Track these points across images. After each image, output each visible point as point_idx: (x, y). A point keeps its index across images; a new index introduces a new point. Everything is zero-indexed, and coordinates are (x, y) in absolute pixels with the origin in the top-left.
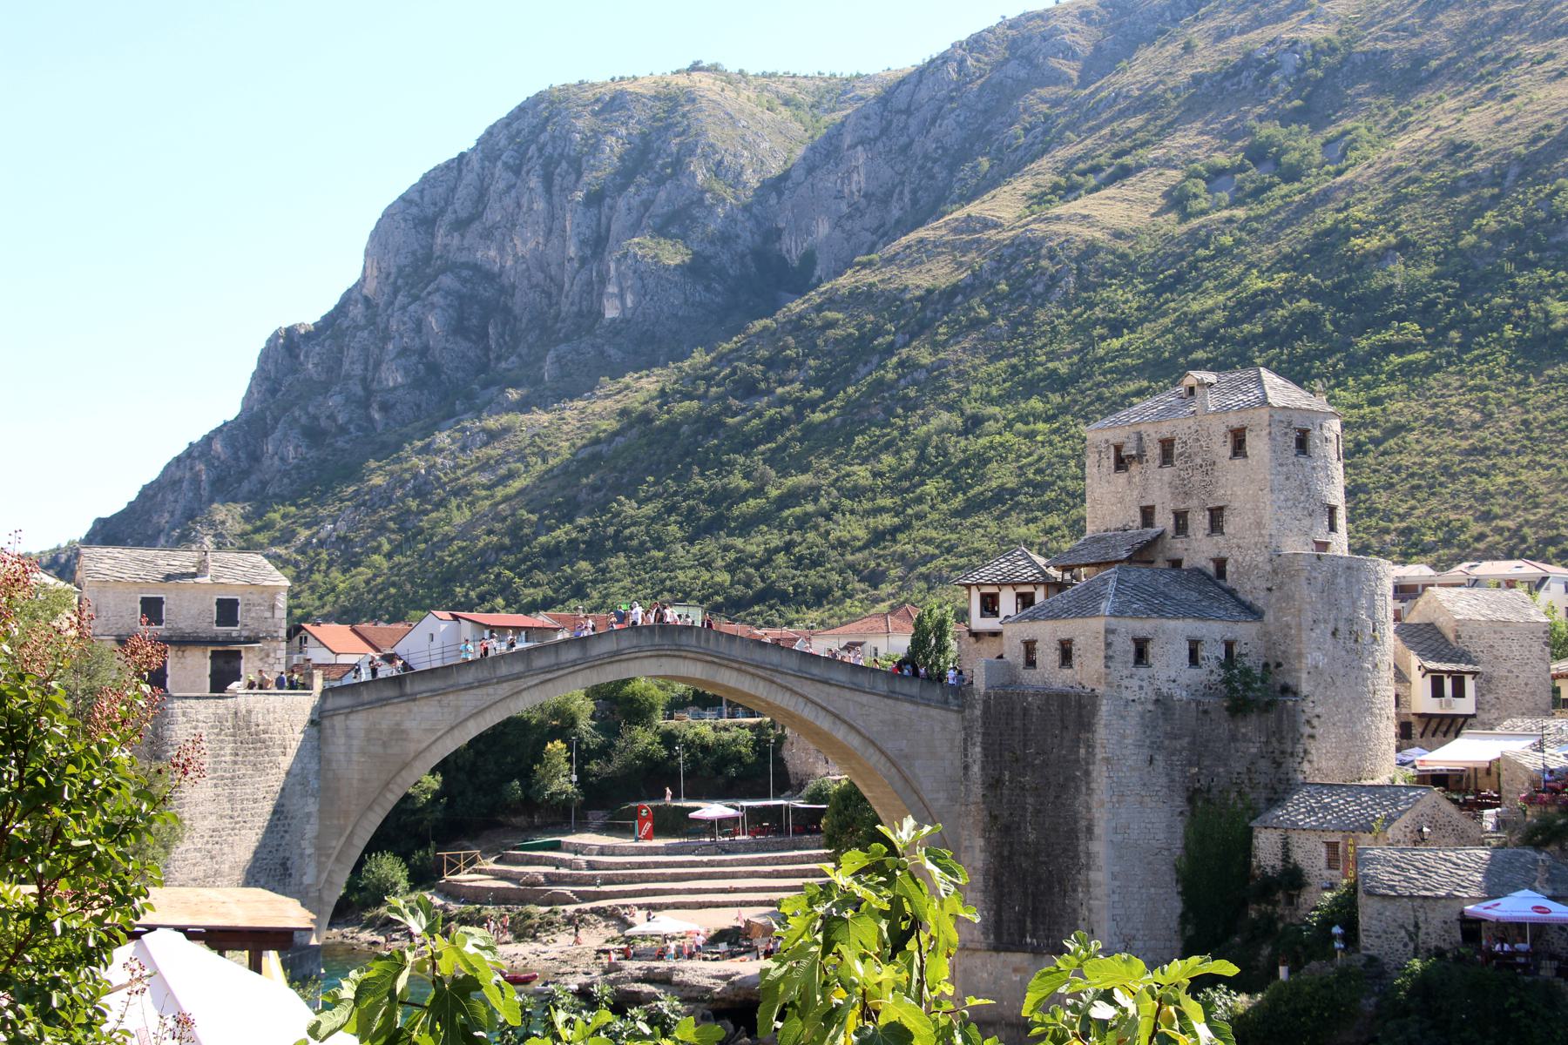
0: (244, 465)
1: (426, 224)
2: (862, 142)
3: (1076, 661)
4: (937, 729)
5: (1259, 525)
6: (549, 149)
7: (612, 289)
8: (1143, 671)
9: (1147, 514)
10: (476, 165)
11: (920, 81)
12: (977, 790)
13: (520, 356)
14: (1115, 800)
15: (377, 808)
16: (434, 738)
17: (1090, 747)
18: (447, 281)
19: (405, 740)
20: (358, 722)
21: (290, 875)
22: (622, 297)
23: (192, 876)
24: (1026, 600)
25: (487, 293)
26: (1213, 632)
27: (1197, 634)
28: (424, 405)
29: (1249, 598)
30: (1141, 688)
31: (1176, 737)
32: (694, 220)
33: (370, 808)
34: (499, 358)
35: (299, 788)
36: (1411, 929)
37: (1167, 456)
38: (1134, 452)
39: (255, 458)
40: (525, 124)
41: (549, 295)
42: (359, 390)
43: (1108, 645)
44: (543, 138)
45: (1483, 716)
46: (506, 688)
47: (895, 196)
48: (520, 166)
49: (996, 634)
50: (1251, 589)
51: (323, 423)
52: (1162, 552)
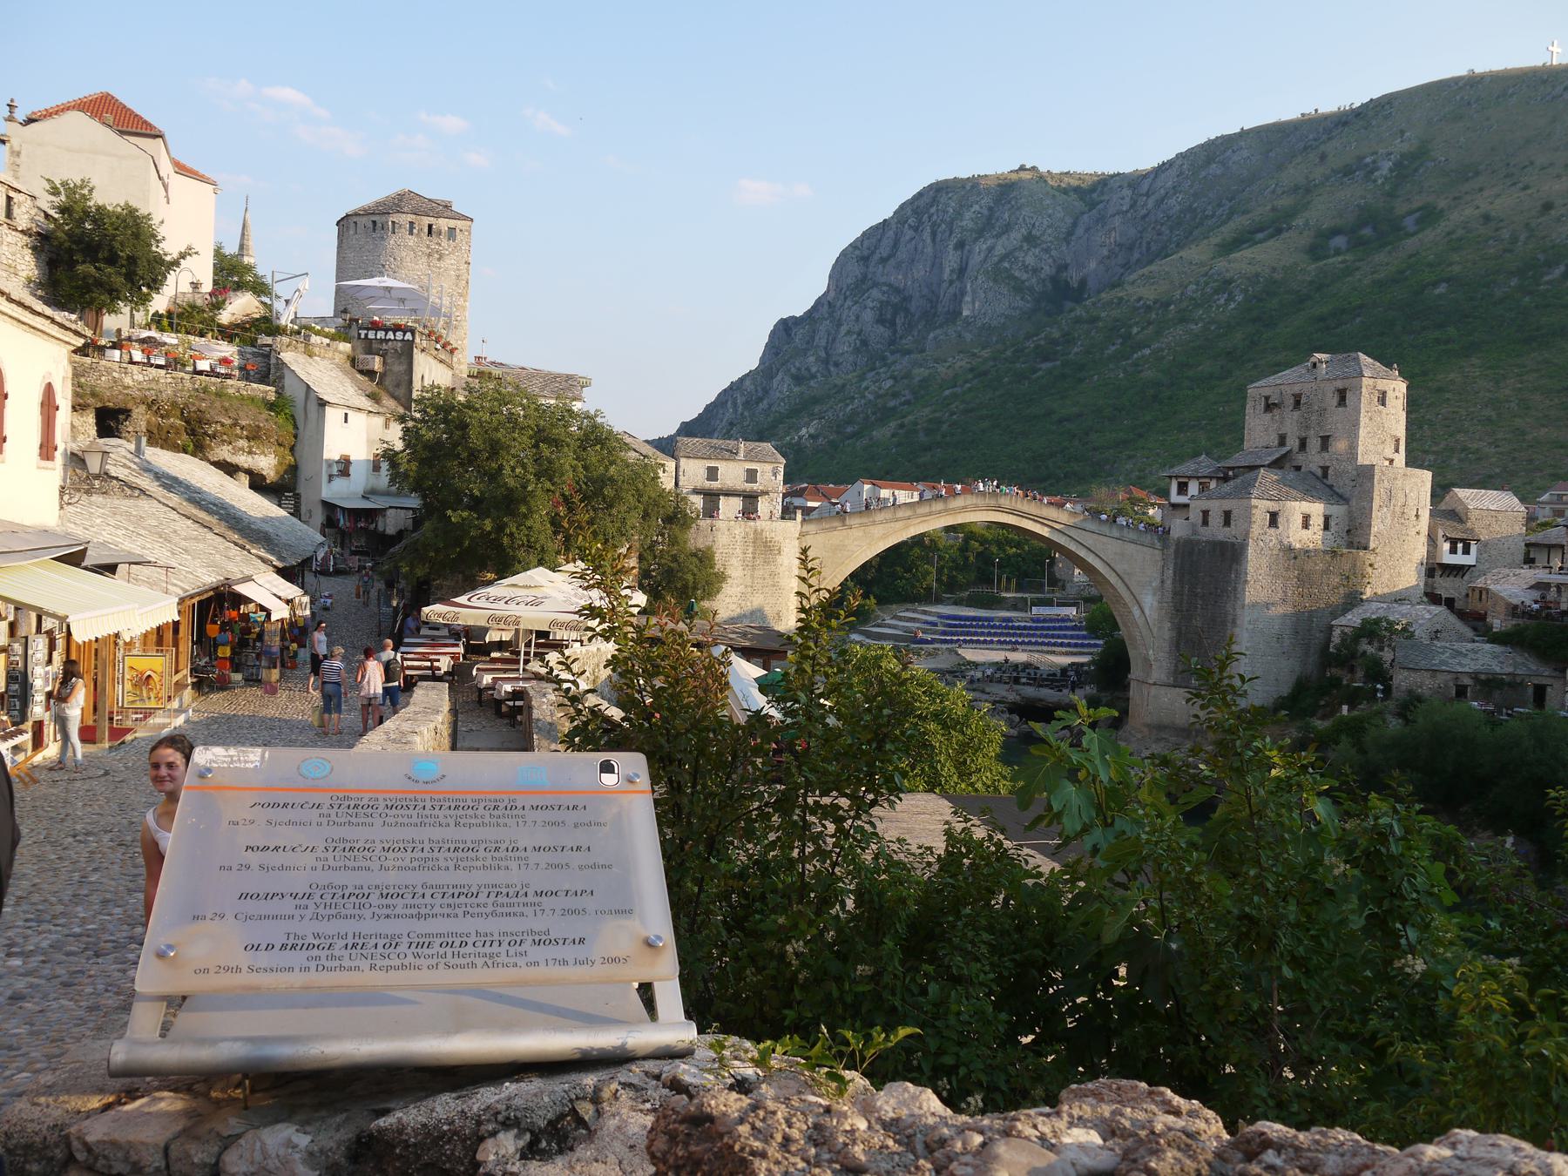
0: (760, 394)
1: (865, 260)
2: (1118, 213)
3: (1232, 523)
7: (968, 298)
8: (1273, 530)
9: (1282, 440)
10: (894, 226)
12: (1169, 595)
18: (875, 293)
22: (973, 303)
24: (1203, 487)
25: (895, 299)
26: (1317, 509)
32: (1016, 258)
37: (1297, 404)
39: (766, 391)
40: (921, 203)
42: (823, 354)
44: (933, 210)
45: (1480, 567)
49: (1186, 506)
50: (1342, 484)
51: (803, 372)
52: (1291, 460)
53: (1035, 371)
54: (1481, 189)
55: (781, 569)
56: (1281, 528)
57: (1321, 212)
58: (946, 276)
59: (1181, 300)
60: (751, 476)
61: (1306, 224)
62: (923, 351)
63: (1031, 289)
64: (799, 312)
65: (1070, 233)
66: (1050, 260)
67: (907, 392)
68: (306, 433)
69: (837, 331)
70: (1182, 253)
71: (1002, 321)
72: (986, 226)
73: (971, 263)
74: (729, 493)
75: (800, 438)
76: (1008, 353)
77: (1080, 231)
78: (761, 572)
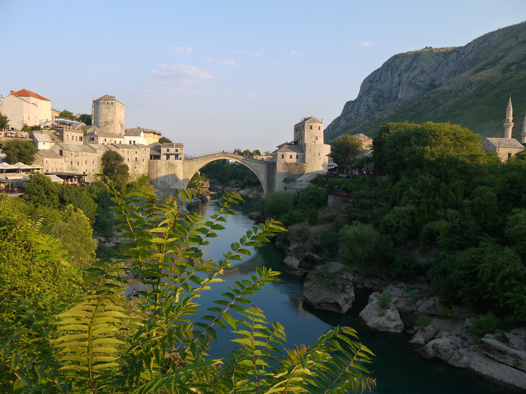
0: (337, 126)
2: (452, 61)
6: (392, 67)
7: (400, 92)
10: (380, 70)
11: (465, 48)
18: (373, 92)
22: (402, 94)
25: (380, 94)
26: (294, 154)
27: (291, 155)
39: (338, 125)
41: (391, 94)
42: (356, 113)
44: (392, 64)
47: (457, 72)
53: (407, 115)
57: (510, 58)
59: (456, 90)
60: (177, 151)
61: (505, 61)
64: (353, 100)
65: (437, 69)
66: (429, 78)
67: (373, 123)
68: (36, 146)
69: (361, 105)
70: (462, 75)
71: (411, 99)
72: (408, 68)
74: (172, 154)
75: (339, 139)
76: (401, 110)
77: (440, 68)
78: (171, 171)
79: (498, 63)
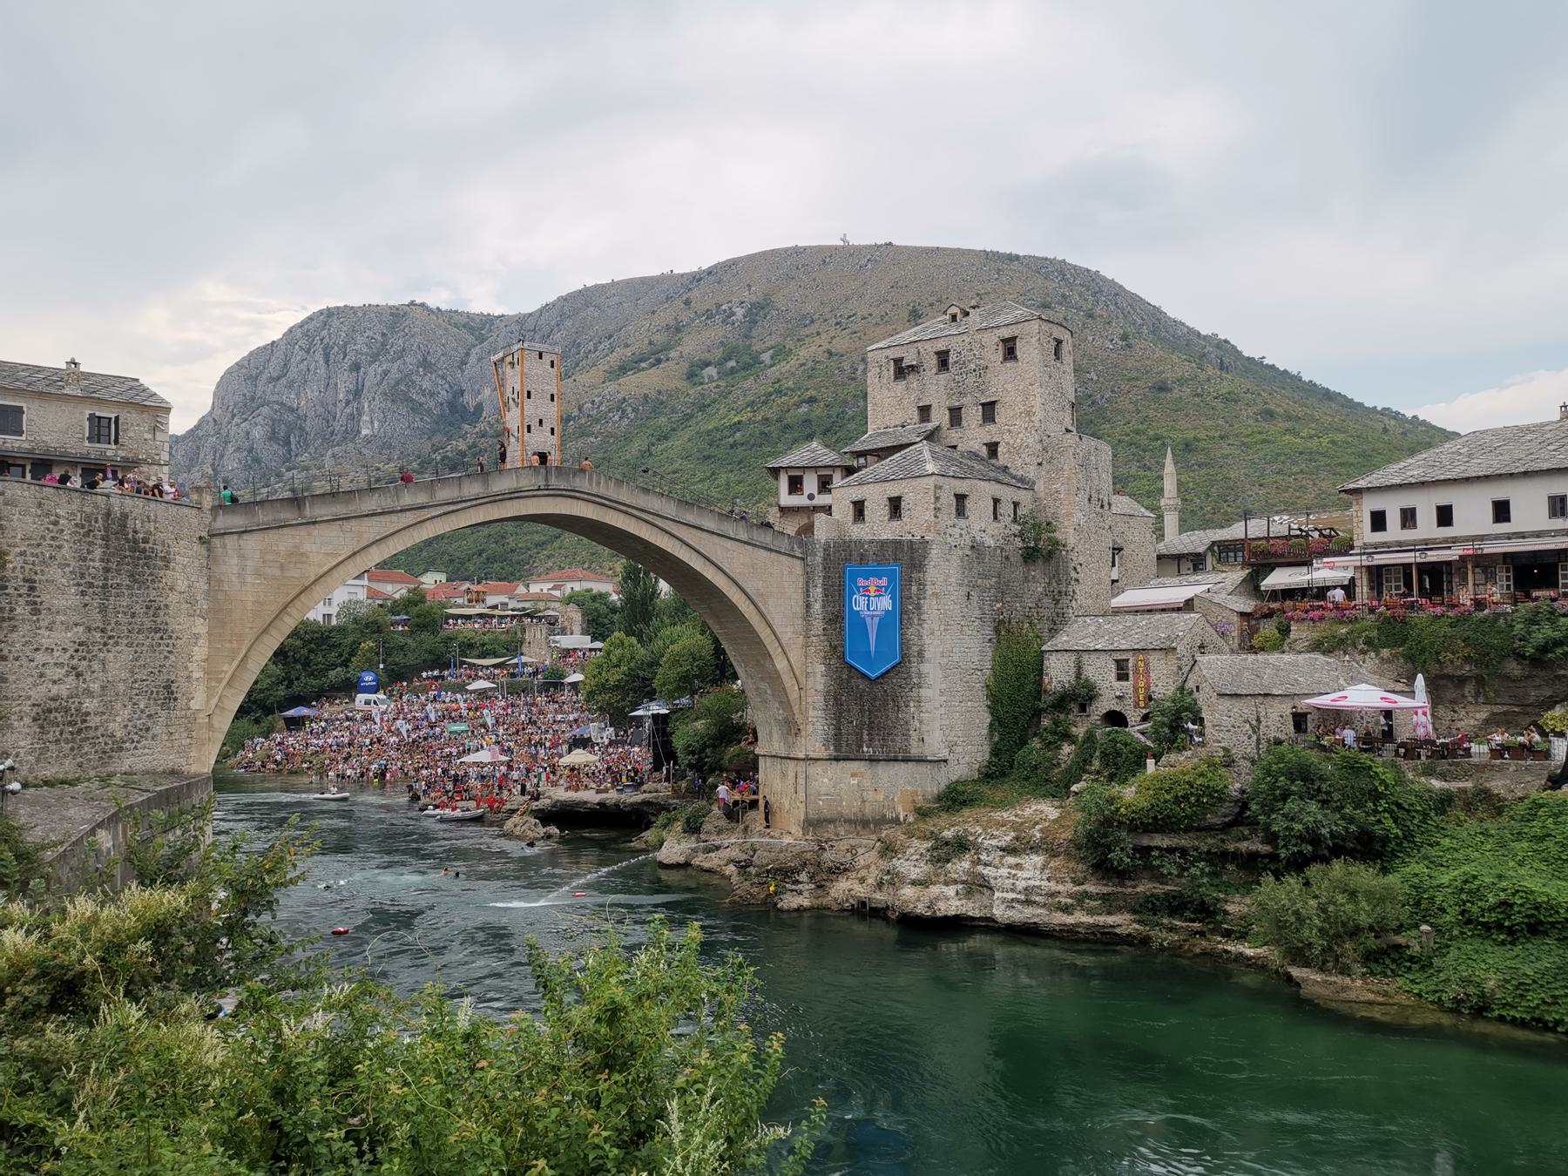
4: (786, 573)
5: (1029, 414)
6: (325, 341)
7: (365, 418)
8: (962, 523)
9: (925, 412)
12: (818, 626)
13: (310, 453)
14: (942, 628)
15: (273, 632)
16: (337, 561)
17: (921, 585)
18: (265, 410)
19: (305, 563)
20: (251, 543)
21: (176, 699)
22: (372, 422)
23: (52, 694)
24: (825, 485)
28: (251, 479)
29: (1020, 473)
30: (961, 535)
31: (986, 577)
32: (414, 382)
33: (265, 631)
34: (296, 455)
35: (186, 606)
36: (1254, 722)
38: (914, 363)
40: (311, 326)
41: (328, 422)
42: (211, 472)
43: (937, 499)
44: (325, 333)
46: (410, 518)
48: (310, 349)
54: (818, 334)
55: (173, 598)
56: (972, 518)
57: (691, 346)
58: (341, 396)
62: (321, 467)
63: (429, 411)
66: (447, 386)
73: (367, 384)
77: (472, 359)
79: (668, 360)
